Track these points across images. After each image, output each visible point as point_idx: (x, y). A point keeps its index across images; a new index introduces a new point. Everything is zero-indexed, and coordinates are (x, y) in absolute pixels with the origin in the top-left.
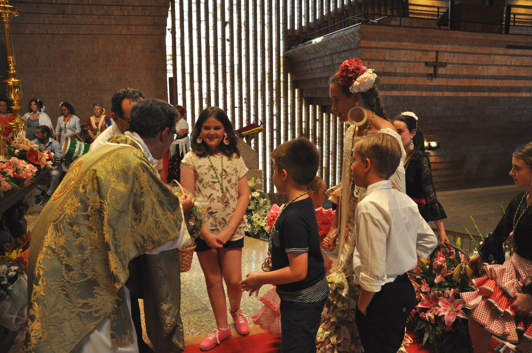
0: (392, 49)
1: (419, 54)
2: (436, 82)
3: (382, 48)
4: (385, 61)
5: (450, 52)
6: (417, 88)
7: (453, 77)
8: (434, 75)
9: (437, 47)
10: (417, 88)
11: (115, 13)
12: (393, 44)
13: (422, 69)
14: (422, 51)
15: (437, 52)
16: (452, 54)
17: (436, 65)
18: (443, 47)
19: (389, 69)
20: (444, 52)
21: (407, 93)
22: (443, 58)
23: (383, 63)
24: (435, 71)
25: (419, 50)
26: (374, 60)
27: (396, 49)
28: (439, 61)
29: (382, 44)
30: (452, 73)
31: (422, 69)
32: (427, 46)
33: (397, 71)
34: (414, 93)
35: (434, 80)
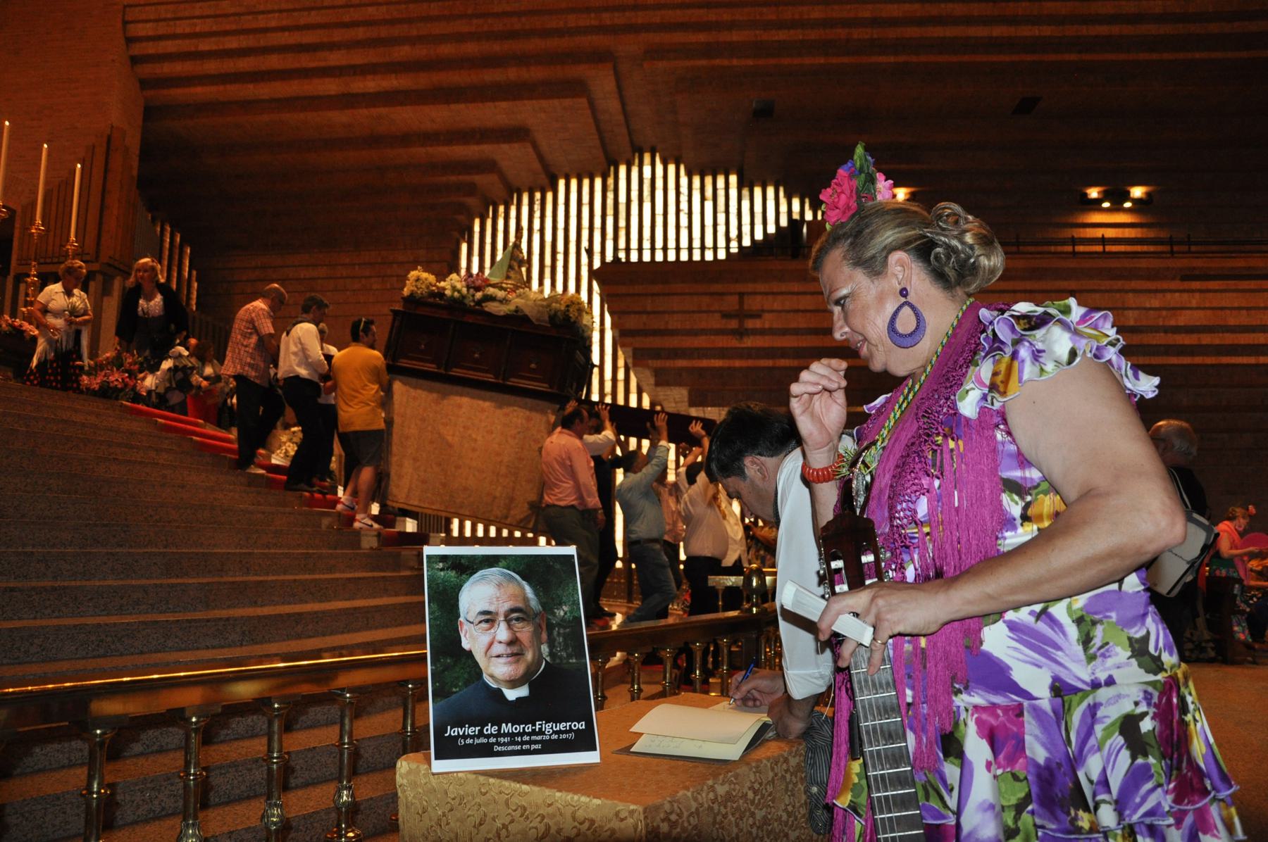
0: (658, 295)
1: (706, 299)
2: (749, 342)
3: (639, 295)
4: (649, 313)
5: (766, 294)
6: (723, 353)
7: (784, 332)
8: (741, 333)
9: (741, 287)
10: (723, 353)
11: (375, 287)
12: (656, 288)
13: (715, 322)
14: (712, 294)
15: (741, 295)
16: (770, 297)
17: (742, 315)
18: (750, 287)
19: (656, 324)
20: (755, 293)
21: (705, 363)
22: (753, 303)
23: (644, 317)
24: (741, 323)
25: (706, 294)
26: (629, 313)
27: (664, 295)
28: (746, 307)
29: (638, 289)
30: (775, 326)
31: (715, 322)
32: (717, 287)
33: (670, 327)
34: (717, 363)
35: (745, 340)
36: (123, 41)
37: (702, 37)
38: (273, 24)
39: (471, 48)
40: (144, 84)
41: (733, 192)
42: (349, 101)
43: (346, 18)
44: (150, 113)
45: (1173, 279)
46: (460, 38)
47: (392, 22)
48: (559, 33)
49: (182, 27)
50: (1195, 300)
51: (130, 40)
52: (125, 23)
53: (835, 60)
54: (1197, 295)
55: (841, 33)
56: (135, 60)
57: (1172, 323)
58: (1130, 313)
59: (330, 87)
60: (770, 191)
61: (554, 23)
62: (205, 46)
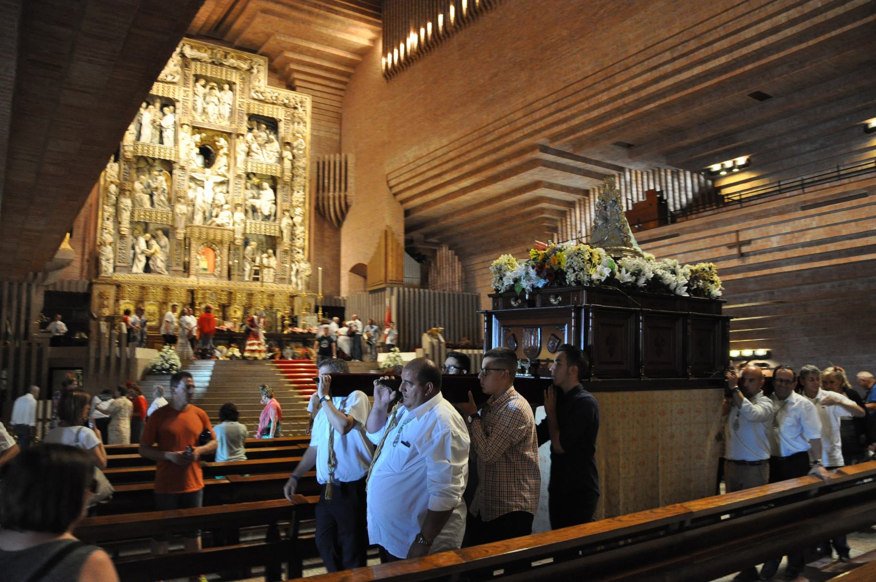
36: (388, 189)
37: (564, 126)
38: (425, 169)
39: (487, 160)
40: (402, 202)
41: (669, 178)
42: (464, 191)
43: (444, 160)
44: (407, 213)
45: (796, 210)
46: (482, 156)
47: (459, 156)
48: (513, 143)
49: (402, 178)
50: (814, 222)
51: (391, 188)
52: (388, 181)
53: (626, 116)
54: (816, 218)
55: (620, 102)
56: (395, 195)
57: (802, 241)
58: (774, 239)
59: (453, 188)
60: (688, 173)
61: (508, 140)
62: (410, 184)
